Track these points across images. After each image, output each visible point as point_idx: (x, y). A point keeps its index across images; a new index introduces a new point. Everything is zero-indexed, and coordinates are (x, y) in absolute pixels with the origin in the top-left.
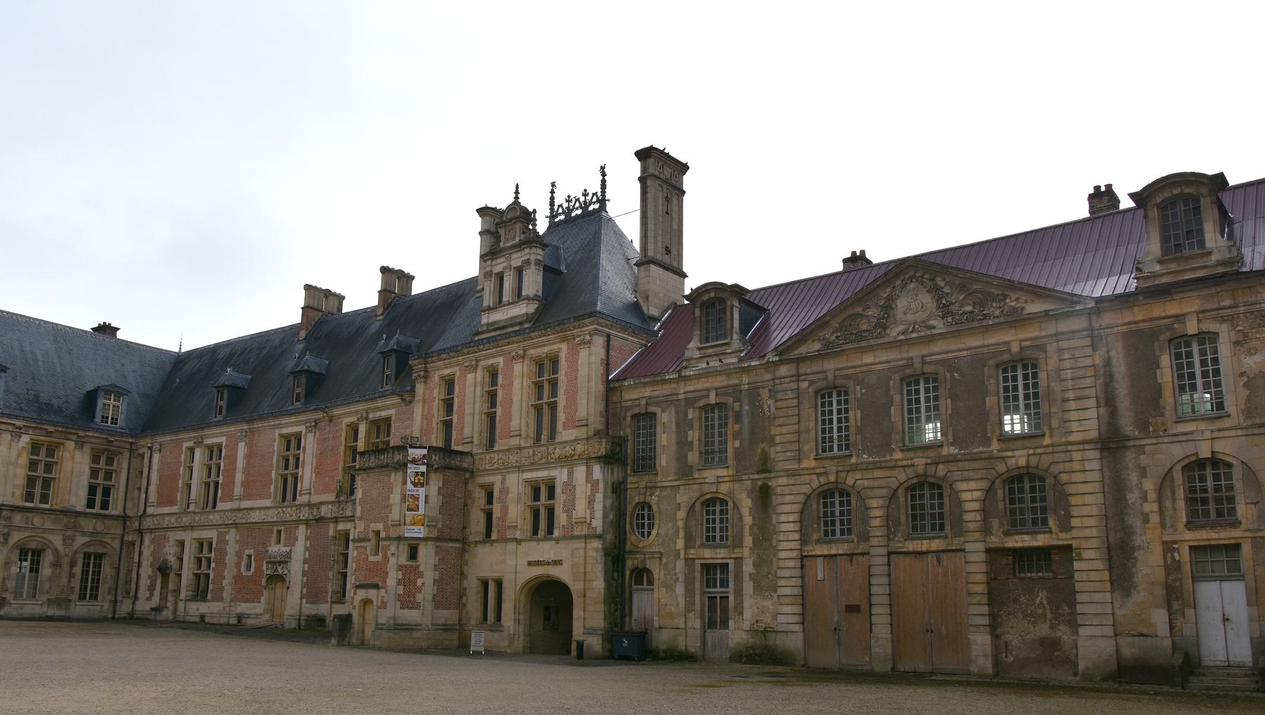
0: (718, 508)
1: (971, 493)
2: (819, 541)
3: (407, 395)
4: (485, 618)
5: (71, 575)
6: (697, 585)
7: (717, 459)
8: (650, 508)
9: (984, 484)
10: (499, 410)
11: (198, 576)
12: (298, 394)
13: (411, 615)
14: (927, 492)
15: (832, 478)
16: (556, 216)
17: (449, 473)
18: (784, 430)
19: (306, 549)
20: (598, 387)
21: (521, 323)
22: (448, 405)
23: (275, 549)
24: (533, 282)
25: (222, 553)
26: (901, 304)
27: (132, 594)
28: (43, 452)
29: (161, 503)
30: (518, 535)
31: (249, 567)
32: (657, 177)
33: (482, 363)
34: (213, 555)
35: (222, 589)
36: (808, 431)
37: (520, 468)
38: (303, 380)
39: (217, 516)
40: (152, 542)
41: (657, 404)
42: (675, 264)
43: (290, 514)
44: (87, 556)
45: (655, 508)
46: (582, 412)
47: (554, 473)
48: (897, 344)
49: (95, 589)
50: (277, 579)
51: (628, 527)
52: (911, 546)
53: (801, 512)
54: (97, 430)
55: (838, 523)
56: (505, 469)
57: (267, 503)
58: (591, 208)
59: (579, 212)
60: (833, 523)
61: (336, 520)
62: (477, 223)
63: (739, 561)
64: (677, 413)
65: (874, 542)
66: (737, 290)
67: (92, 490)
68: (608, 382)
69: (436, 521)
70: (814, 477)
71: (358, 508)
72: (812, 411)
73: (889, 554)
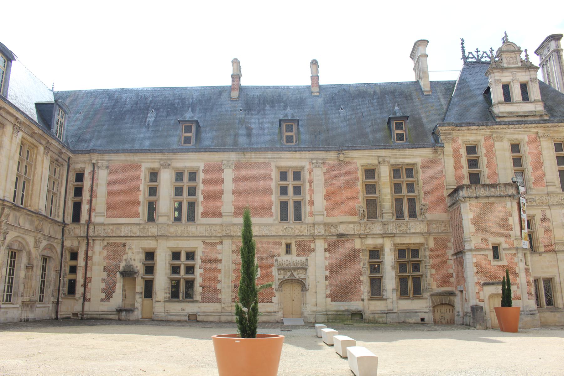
19: (326, 259)
23: (284, 259)
29: (110, 214)
33: (508, 136)
40: (104, 249)
61: (366, 236)
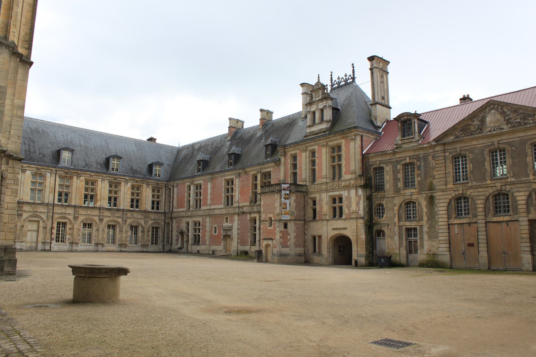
0: (411, 205)
1: (521, 197)
2: (456, 218)
3: (278, 163)
4: (315, 251)
5: (148, 235)
6: (404, 237)
7: (410, 185)
8: (382, 206)
9: (527, 193)
10: (317, 167)
11: (195, 236)
12: (231, 163)
13: (286, 250)
14: (501, 197)
15: (461, 192)
16: (334, 85)
17: (298, 194)
18: (439, 173)
19: (238, 224)
20: (359, 157)
21: (324, 132)
22: (295, 166)
24: (328, 115)
25: (205, 226)
26: (488, 119)
27: (170, 242)
28: (135, 188)
30: (328, 218)
31: (215, 232)
32: (377, 68)
34: (201, 227)
35: (205, 240)
36: (449, 173)
37: (327, 191)
38: (233, 157)
39: (201, 212)
41: (384, 163)
42: (386, 103)
43: (231, 211)
44: (153, 228)
45: (385, 206)
46: (352, 168)
47: (342, 192)
48: (487, 137)
49: (156, 240)
50: (227, 237)
51: (374, 214)
52: (495, 219)
53: (448, 206)
54: (153, 179)
55: (463, 211)
56: (320, 191)
57: (222, 206)
58: (348, 81)
59: (344, 83)
60: (461, 210)
61: (250, 213)
62: (301, 90)
63: (421, 226)
64: (393, 167)
65: (479, 218)
66: (416, 115)
67: (153, 202)
68: (362, 155)
69: (293, 213)
70: (453, 192)
71: (262, 208)
72: (451, 165)
73: (486, 223)
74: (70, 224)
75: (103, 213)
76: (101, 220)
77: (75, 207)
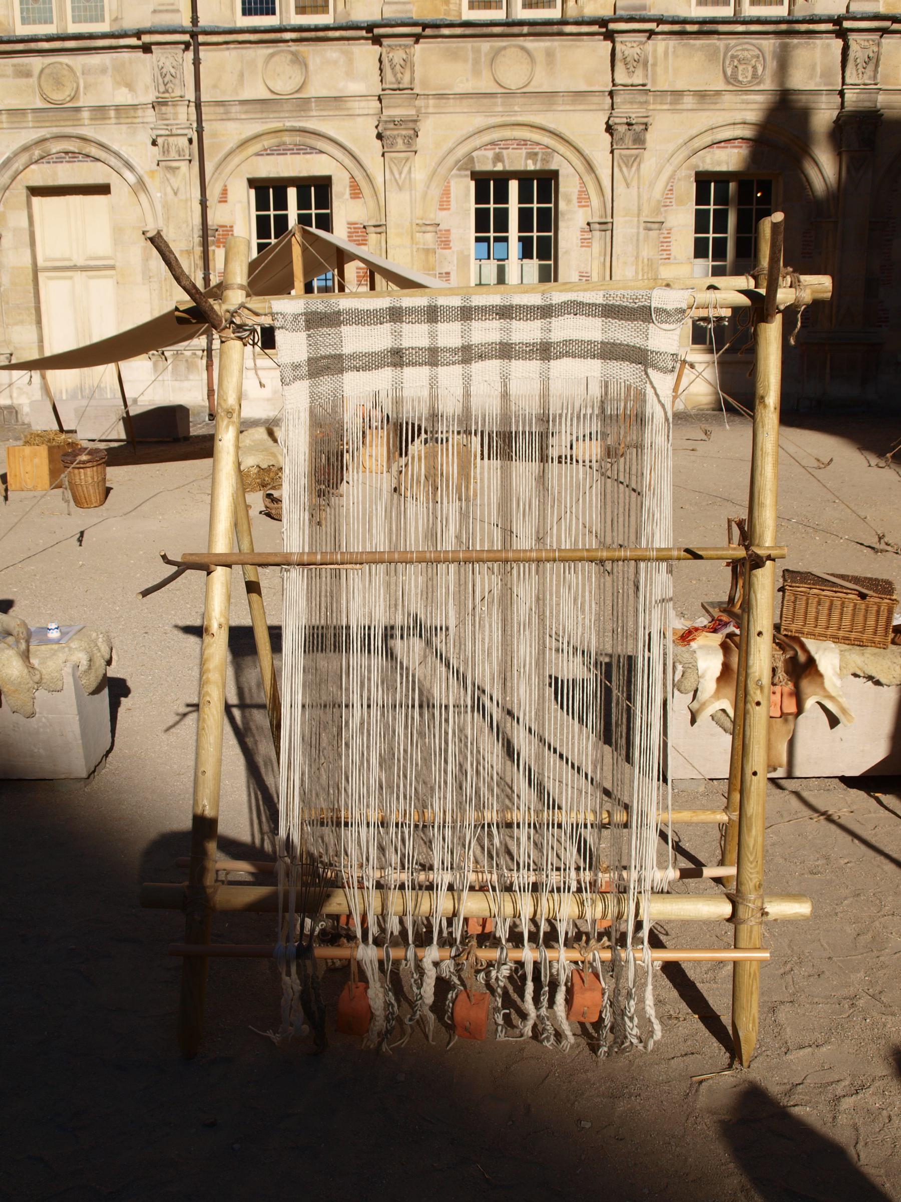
74: (356, 192)
75: (642, 62)
76: (626, 135)
77: (373, 33)
